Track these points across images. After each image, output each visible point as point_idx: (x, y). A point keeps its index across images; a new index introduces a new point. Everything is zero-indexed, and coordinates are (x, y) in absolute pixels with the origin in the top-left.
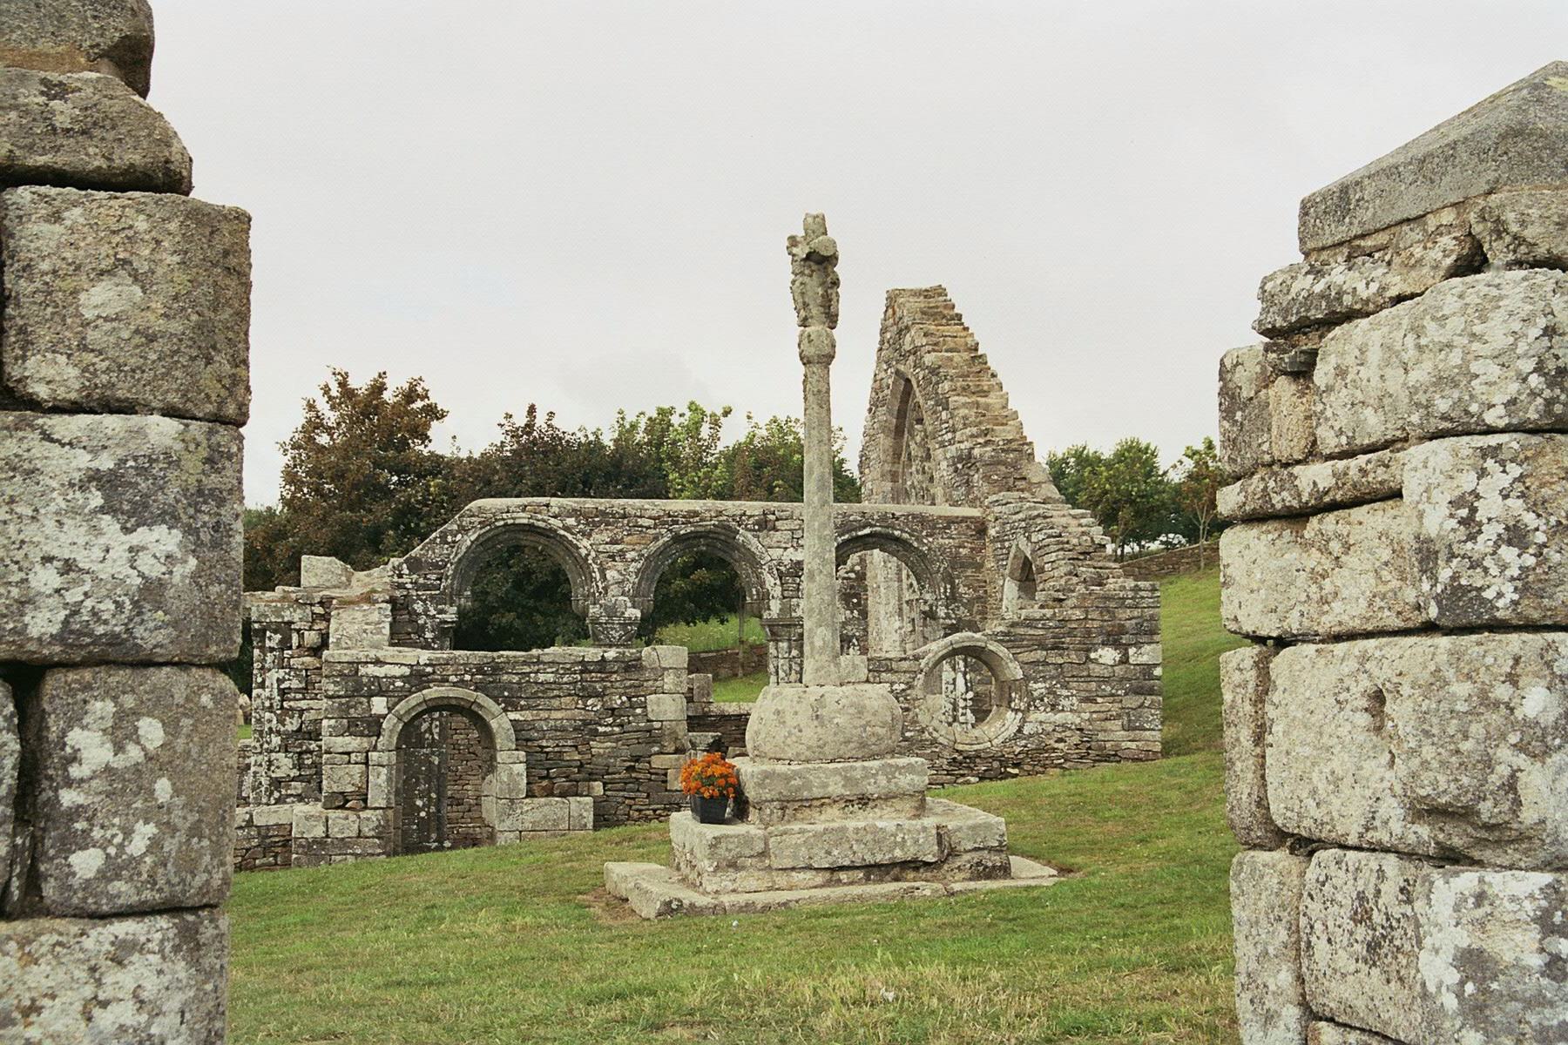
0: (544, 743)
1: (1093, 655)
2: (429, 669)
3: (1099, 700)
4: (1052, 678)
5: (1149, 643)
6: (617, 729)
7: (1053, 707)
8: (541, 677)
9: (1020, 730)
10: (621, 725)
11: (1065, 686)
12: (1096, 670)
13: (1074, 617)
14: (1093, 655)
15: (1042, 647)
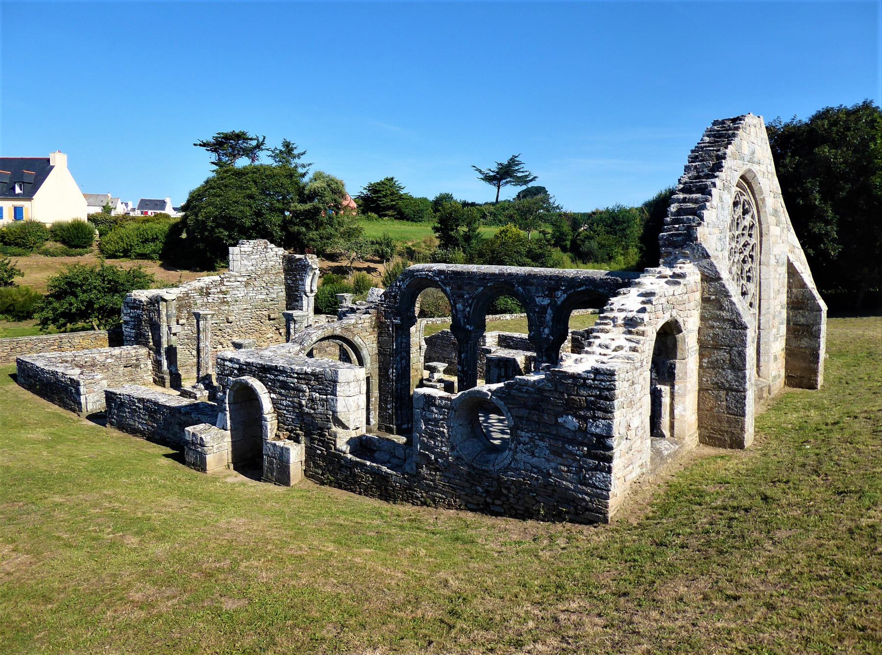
0: (285, 412)
1: (560, 420)
2: (245, 367)
3: (565, 456)
4: (532, 431)
5: (604, 419)
6: (312, 412)
7: (533, 455)
8: (281, 378)
9: (510, 464)
10: (314, 409)
11: (542, 439)
12: (562, 432)
13: (547, 388)
14: (560, 420)
15: (525, 406)
